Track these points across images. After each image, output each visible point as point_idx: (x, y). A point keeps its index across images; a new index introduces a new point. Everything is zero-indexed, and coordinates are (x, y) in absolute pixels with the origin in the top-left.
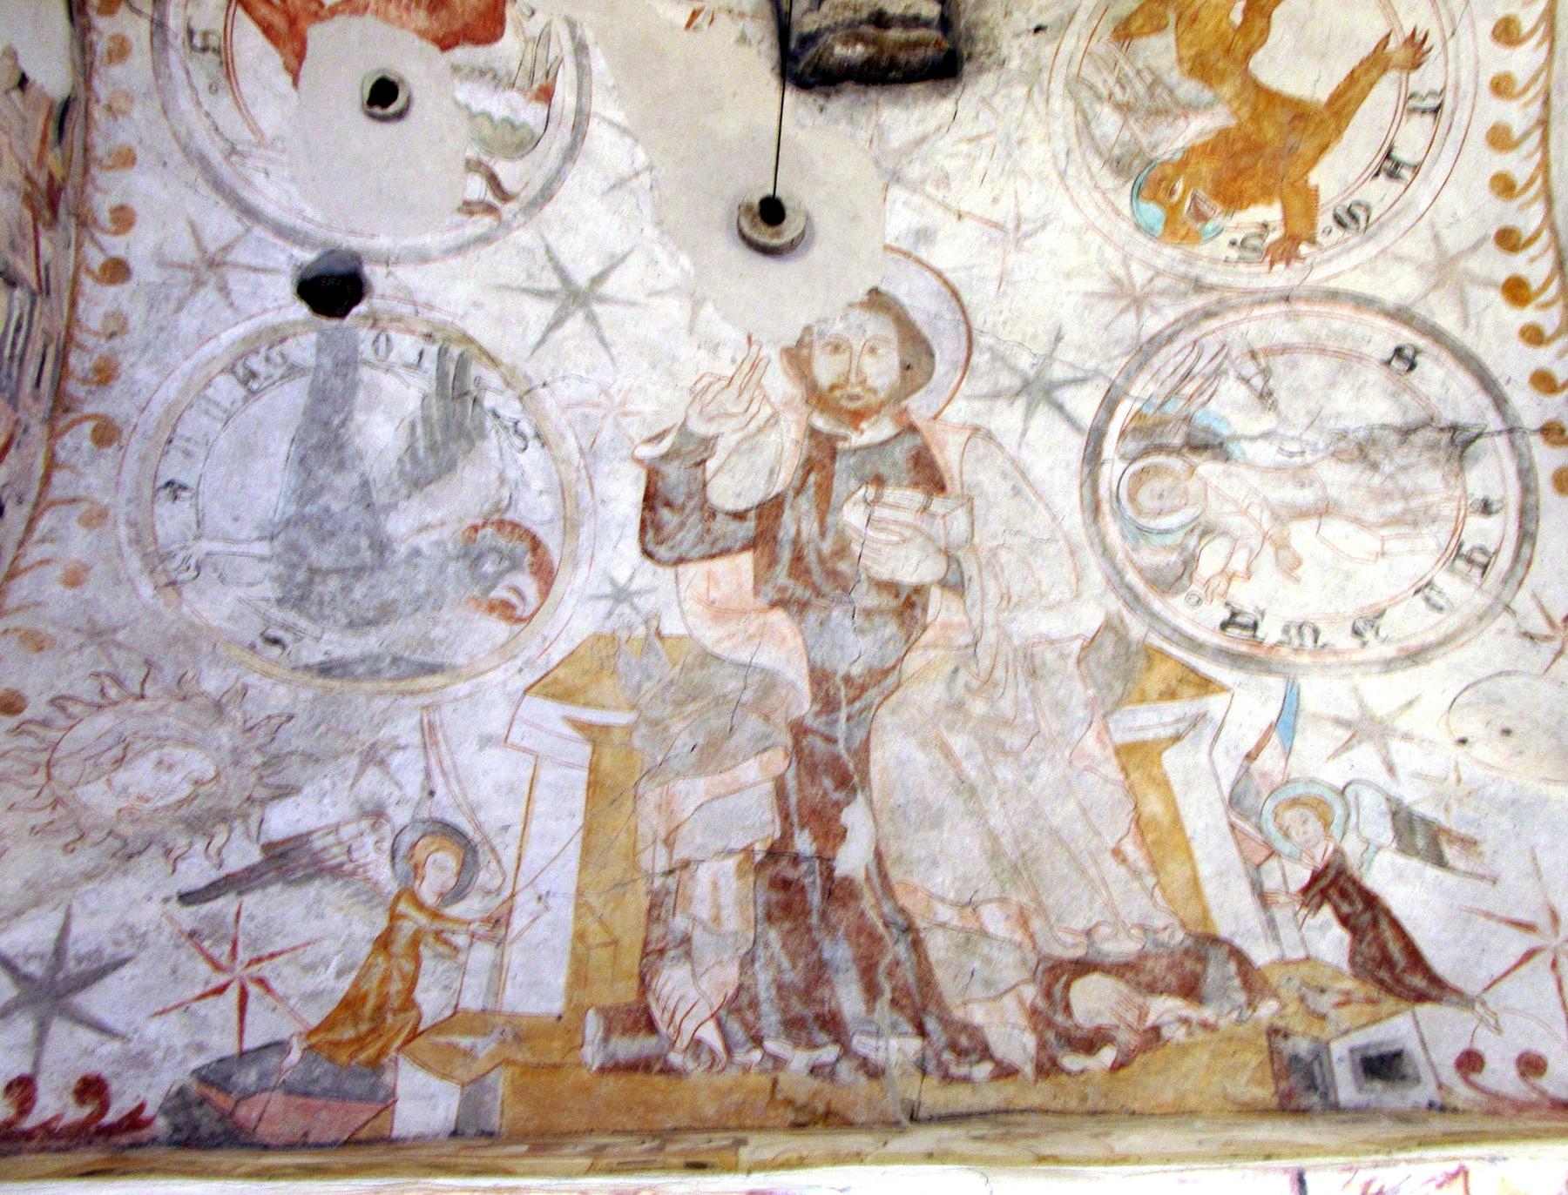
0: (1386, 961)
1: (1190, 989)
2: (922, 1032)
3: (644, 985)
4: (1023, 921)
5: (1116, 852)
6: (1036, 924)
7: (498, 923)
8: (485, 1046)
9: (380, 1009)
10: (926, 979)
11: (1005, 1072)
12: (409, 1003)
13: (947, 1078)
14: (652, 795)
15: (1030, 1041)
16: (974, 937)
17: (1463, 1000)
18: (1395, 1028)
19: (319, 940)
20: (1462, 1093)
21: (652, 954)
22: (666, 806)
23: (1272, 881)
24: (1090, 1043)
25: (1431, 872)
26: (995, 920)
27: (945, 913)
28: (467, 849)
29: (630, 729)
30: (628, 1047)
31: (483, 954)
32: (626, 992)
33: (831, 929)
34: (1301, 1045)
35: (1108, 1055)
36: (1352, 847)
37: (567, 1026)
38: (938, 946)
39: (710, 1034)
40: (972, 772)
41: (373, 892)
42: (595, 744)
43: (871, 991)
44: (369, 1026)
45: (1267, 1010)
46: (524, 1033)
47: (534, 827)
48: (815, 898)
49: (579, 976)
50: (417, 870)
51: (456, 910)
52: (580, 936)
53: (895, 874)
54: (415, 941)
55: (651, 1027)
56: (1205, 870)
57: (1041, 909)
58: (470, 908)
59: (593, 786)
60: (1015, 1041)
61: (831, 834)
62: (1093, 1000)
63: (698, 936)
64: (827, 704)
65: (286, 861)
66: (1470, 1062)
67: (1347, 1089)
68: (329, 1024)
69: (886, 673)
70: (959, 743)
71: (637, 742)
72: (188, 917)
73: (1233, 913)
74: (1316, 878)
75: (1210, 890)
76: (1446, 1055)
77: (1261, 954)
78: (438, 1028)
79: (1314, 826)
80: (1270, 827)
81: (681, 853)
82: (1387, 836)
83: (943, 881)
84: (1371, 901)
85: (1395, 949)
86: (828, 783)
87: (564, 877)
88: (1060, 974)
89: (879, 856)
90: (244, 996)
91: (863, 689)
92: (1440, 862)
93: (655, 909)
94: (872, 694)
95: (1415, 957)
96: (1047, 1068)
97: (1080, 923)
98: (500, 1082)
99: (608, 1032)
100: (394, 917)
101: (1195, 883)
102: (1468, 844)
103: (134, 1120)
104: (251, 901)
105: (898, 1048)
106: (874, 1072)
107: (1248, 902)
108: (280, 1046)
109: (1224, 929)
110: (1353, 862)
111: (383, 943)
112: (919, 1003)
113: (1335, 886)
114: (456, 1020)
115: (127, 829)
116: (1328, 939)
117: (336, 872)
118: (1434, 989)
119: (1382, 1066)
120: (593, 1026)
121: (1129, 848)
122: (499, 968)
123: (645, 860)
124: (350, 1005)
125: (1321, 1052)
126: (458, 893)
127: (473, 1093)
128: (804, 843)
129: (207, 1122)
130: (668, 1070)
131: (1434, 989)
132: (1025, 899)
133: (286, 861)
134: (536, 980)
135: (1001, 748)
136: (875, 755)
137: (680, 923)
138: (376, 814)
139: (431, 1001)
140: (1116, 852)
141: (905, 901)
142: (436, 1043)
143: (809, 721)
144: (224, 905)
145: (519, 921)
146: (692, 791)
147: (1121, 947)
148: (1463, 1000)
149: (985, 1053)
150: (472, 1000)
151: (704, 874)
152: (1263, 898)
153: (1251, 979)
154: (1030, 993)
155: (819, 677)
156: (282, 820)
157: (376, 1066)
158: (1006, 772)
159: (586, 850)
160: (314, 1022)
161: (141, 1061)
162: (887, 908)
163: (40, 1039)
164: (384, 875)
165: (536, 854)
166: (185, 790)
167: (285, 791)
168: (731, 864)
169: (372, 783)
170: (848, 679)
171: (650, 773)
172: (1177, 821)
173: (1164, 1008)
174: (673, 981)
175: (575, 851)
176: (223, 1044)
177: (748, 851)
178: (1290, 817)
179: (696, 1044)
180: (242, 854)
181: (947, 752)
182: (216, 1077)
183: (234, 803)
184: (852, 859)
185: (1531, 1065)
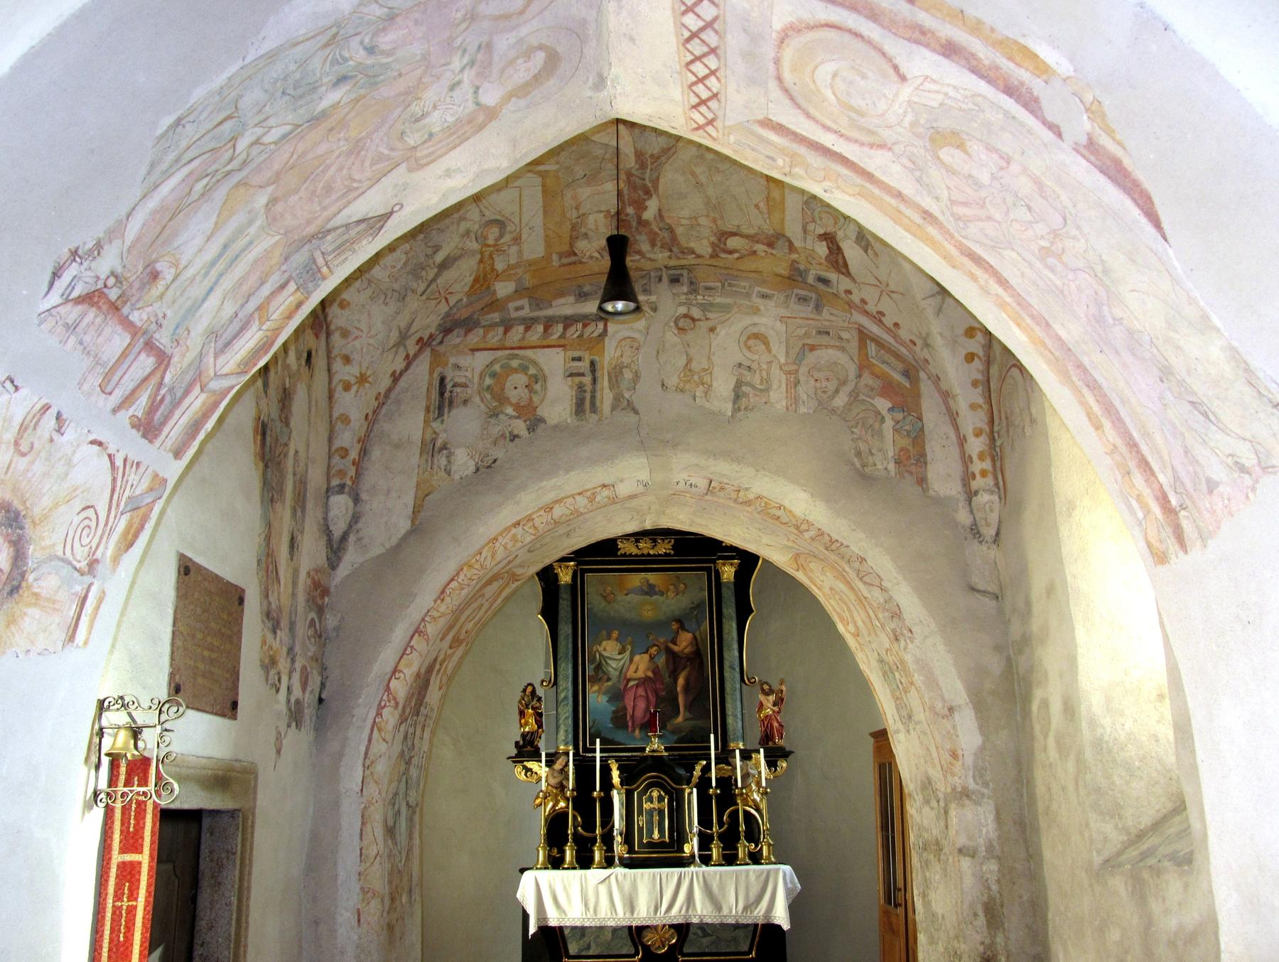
0: (837, 262)
1: (771, 245)
2: (671, 251)
3: (571, 246)
4: (715, 221)
5: (757, 206)
6: (719, 222)
7: (517, 240)
8: (520, 271)
9: (485, 276)
10: (674, 239)
11: (698, 256)
12: (493, 269)
13: (678, 258)
14: (568, 194)
15: (710, 250)
16: (694, 224)
17: (854, 280)
18: (832, 276)
19: (461, 277)
20: (843, 295)
21: (573, 239)
22: (574, 198)
23: (811, 227)
24: (731, 252)
25: (862, 252)
26: (703, 221)
27: (684, 222)
28: (501, 224)
29: (557, 171)
30: (565, 261)
31: (514, 249)
32: (566, 248)
33: (640, 233)
34: (802, 267)
35: (736, 255)
36: (840, 234)
37: (547, 258)
38: (679, 231)
39: (596, 255)
40: (703, 179)
41: (473, 253)
42: (543, 177)
43: (653, 244)
44: (483, 281)
45: (794, 256)
46: (531, 263)
47: (524, 209)
48: (634, 224)
49: (548, 243)
50: (486, 238)
51: (502, 241)
52: (547, 236)
53: (665, 214)
54: (491, 256)
55: (575, 254)
56: (787, 218)
57: (722, 218)
58: (507, 238)
59: (544, 192)
60: (704, 248)
61: (640, 206)
62: (733, 243)
63: (590, 233)
64: (643, 166)
65: (444, 266)
66: (849, 292)
67: (811, 280)
68: (472, 287)
69: (669, 149)
70: (698, 170)
71: (560, 174)
72: (424, 297)
73: (793, 230)
74: (825, 234)
75: (787, 224)
76: (842, 288)
77: (797, 244)
78: (504, 271)
79: (831, 221)
80: (816, 214)
81: (581, 212)
82: (854, 238)
83: (686, 213)
84: (839, 249)
85: (841, 261)
86: (641, 192)
87: (539, 220)
88: (724, 235)
89: (660, 210)
90: (446, 299)
91: (658, 158)
92: (866, 251)
93: (574, 228)
94: (663, 159)
95: (846, 265)
96: (714, 256)
97: (736, 223)
98: (527, 276)
99: (560, 258)
100: (482, 253)
101: (783, 220)
102: (876, 254)
103: (431, 336)
104: (439, 281)
105: (661, 257)
106: (650, 259)
107: (799, 229)
108: (461, 300)
109: (788, 234)
110: (838, 238)
111: (481, 261)
112: (672, 244)
113: (829, 238)
114: (510, 267)
115: (396, 286)
116: (822, 249)
117: (460, 257)
118: (848, 273)
119: (825, 281)
120: (555, 257)
121: (762, 205)
122: (520, 251)
123: (568, 215)
124: (476, 280)
125: (807, 271)
126: (501, 236)
127: (519, 281)
128: (630, 210)
129: (448, 325)
130: (581, 263)
131: (848, 273)
132: (717, 216)
133: (444, 266)
134: (534, 247)
135: (718, 170)
136: (661, 180)
137: (583, 230)
138: (468, 233)
139: (500, 266)
140: (757, 206)
141: (668, 221)
142: (505, 275)
143: (634, 171)
144: (433, 286)
145: (524, 237)
146: (584, 192)
147: (752, 232)
148: (854, 280)
149: (693, 252)
150: (512, 262)
151: (591, 218)
152: (805, 231)
153: (791, 247)
154: (713, 239)
155: (639, 155)
156: (440, 257)
157: (489, 288)
158: (718, 178)
159: (545, 212)
160: (467, 289)
161: (428, 326)
162: (661, 225)
163: (405, 346)
164: (475, 246)
165: (525, 218)
166: (404, 257)
167: (437, 248)
168: (602, 215)
169: (464, 226)
170: (652, 156)
171: (568, 186)
172: (783, 202)
173: (760, 248)
174: (582, 245)
175: (541, 212)
176: (447, 309)
177: (608, 212)
178: (824, 215)
179: (591, 257)
180: (432, 273)
181: (693, 174)
182: (447, 315)
183: (422, 259)
184: (649, 215)
185: (863, 301)
